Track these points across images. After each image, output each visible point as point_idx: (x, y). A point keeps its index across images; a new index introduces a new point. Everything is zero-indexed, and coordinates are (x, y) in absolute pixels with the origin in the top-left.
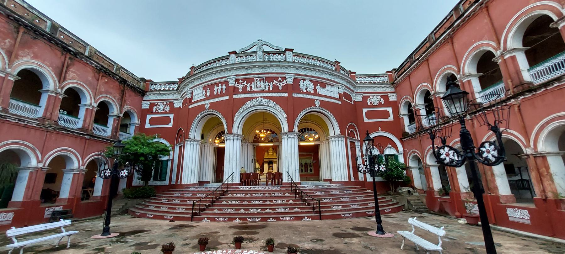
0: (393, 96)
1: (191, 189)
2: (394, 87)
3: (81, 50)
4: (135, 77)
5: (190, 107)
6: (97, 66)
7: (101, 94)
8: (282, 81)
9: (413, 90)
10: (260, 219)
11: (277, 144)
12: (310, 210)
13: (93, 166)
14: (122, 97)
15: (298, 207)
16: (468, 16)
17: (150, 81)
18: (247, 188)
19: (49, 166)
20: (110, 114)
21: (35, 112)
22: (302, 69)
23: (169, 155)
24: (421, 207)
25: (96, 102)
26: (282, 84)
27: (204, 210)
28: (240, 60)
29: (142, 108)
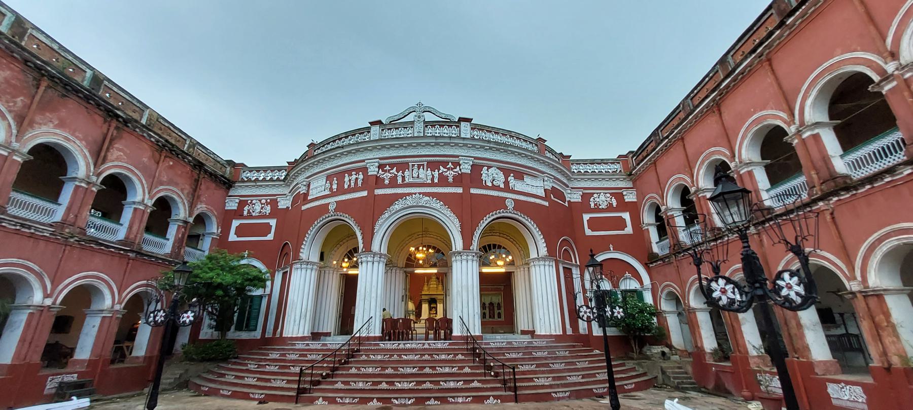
0: (631, 195)
1: (297, 347)
2: (631, 179)
3: (136, 116)
4: (219, 159)
5: (304, 208)
6: (158, 141)
7: (162, 184)
9: (662, 186)
10: (414, 400)
11: (443, 270)
12: (499, 385)
13: (136, 305)
14: (195, 190)
15: (479, 378)
16: (742, 73)
17: (243, 165)
18: (393, 344)
19: (62, 303)
20: (173, 217)
21: (50, 213)
22: (486, 149)
23: (264, 287)
24: (685, 381)
25: (151, 198)
26: (453, 173)
27: (319, 383)
28: (387, 134)
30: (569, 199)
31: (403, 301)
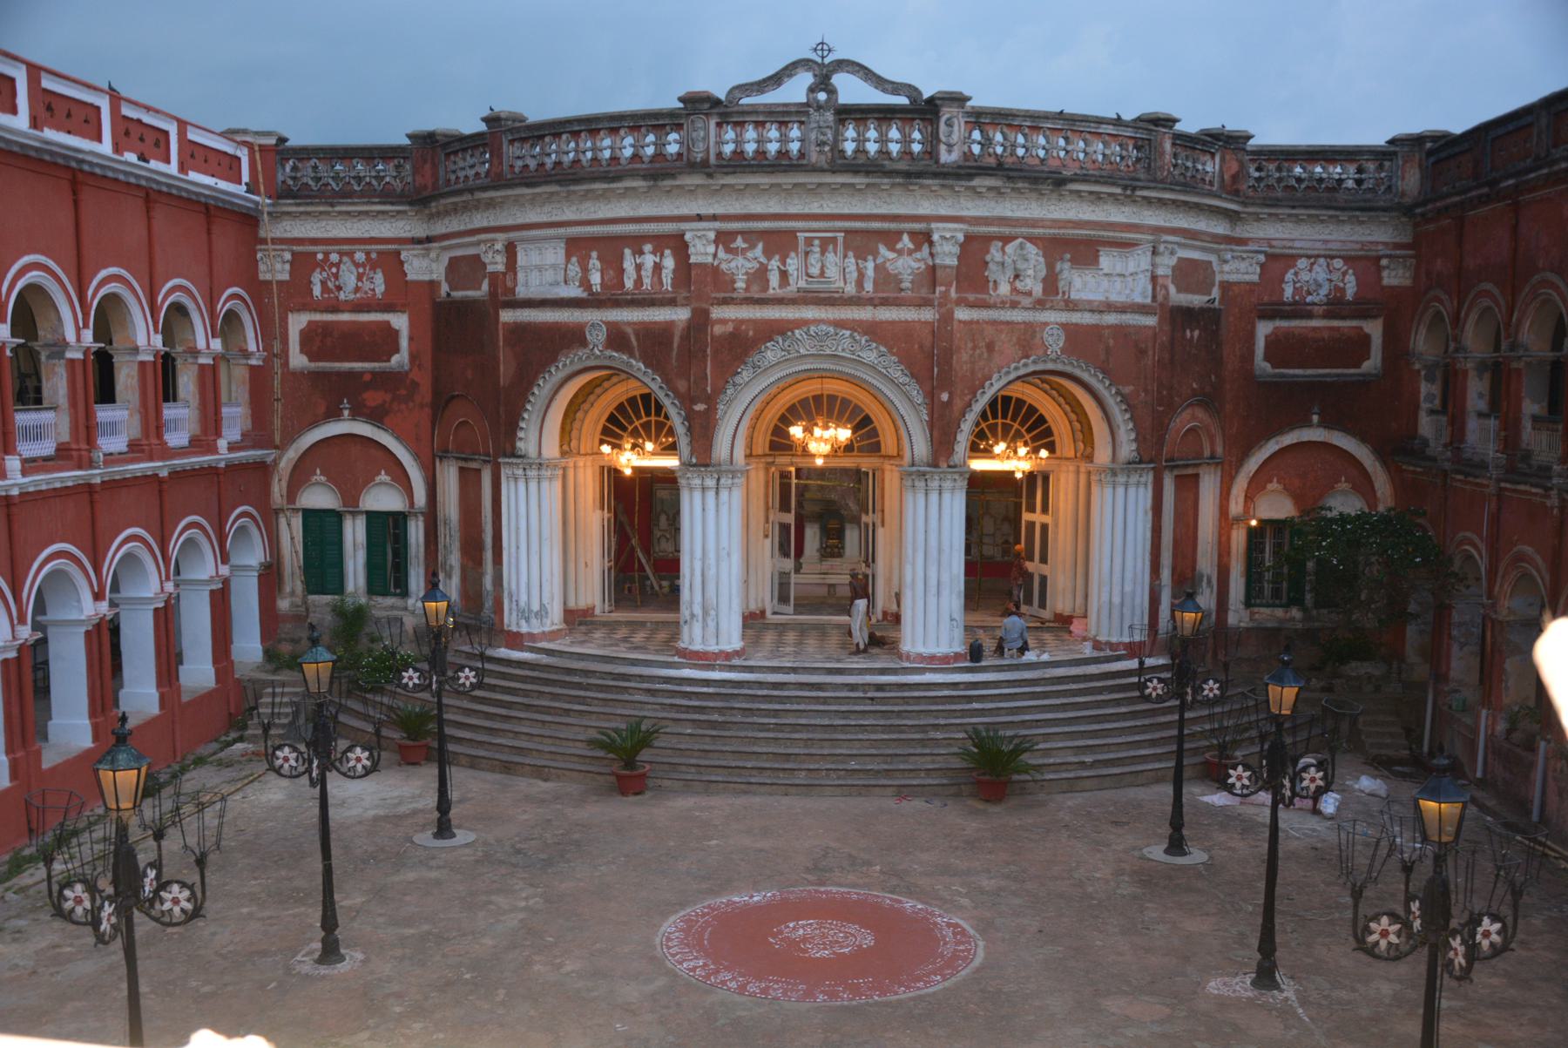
29: (262, 277)
30: (1226, 277)
31: (766, 536)
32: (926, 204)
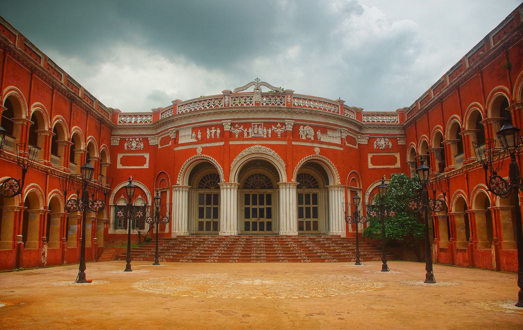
5: (176, 149)
8: (281, 127)
26: (281, 130)
29: (111, 144)
32: (284, 116)
